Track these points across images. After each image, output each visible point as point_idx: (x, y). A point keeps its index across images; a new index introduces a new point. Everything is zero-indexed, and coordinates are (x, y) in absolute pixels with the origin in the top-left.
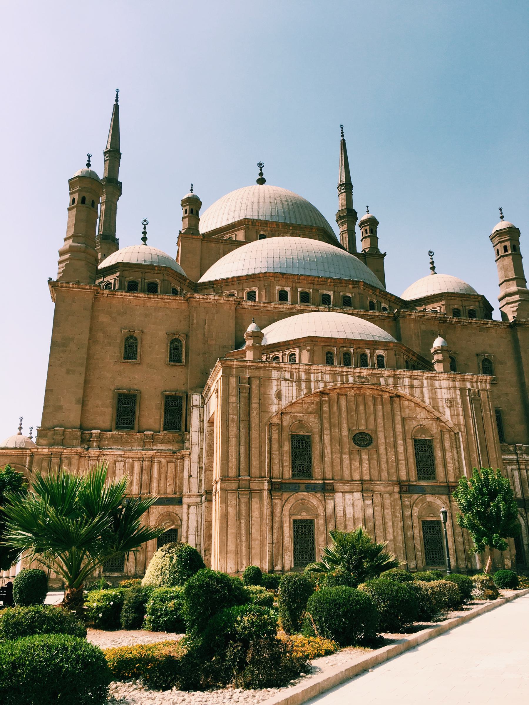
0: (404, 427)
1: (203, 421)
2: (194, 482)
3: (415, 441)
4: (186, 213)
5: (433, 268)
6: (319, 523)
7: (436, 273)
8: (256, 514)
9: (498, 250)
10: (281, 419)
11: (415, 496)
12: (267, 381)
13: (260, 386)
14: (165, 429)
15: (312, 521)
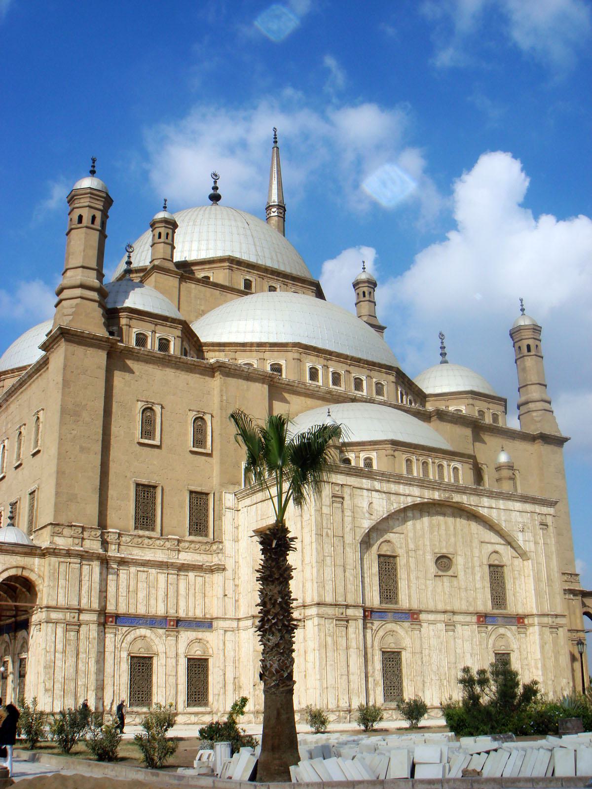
0: (481, 552)
1: (237, 528)
2: (230, 602)
3: (490, 566)
4: (160, 237)
5: (443, 355)
6: (404, 656)
7: (446, 362)
8: (353, 644)
9: (520, 348)
10: (369, 536)
11: (490, 628)
12: (359, 490)
13: (352, 496)
14: (190, 534)
15: (399, 653)
